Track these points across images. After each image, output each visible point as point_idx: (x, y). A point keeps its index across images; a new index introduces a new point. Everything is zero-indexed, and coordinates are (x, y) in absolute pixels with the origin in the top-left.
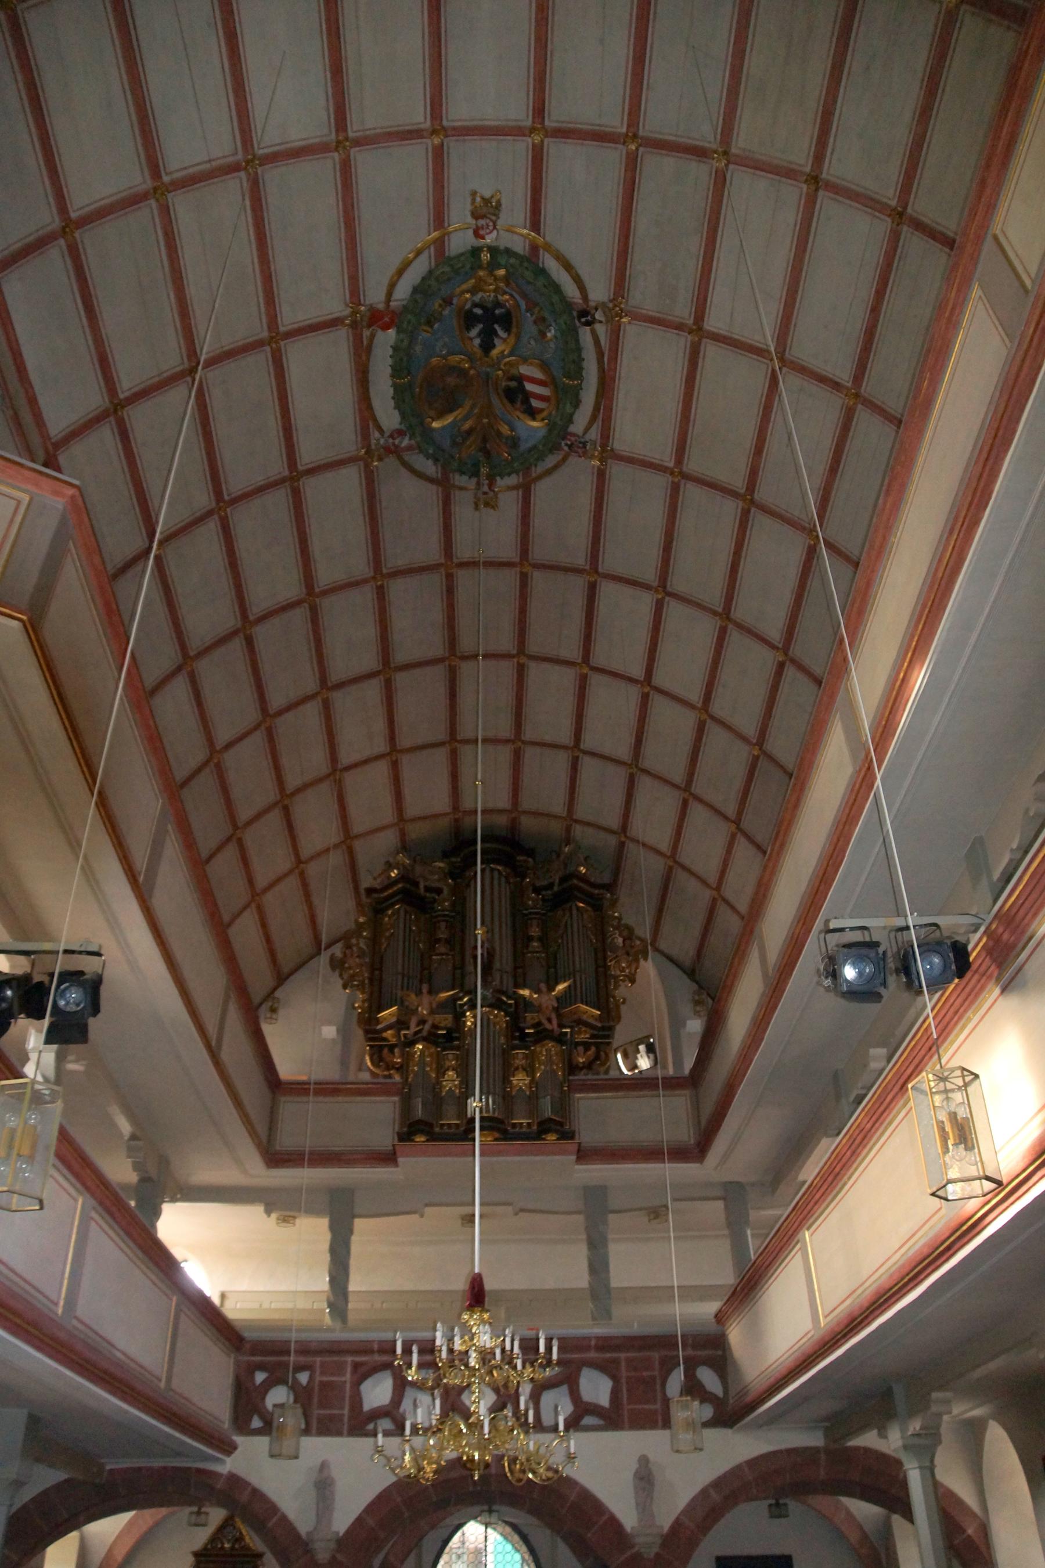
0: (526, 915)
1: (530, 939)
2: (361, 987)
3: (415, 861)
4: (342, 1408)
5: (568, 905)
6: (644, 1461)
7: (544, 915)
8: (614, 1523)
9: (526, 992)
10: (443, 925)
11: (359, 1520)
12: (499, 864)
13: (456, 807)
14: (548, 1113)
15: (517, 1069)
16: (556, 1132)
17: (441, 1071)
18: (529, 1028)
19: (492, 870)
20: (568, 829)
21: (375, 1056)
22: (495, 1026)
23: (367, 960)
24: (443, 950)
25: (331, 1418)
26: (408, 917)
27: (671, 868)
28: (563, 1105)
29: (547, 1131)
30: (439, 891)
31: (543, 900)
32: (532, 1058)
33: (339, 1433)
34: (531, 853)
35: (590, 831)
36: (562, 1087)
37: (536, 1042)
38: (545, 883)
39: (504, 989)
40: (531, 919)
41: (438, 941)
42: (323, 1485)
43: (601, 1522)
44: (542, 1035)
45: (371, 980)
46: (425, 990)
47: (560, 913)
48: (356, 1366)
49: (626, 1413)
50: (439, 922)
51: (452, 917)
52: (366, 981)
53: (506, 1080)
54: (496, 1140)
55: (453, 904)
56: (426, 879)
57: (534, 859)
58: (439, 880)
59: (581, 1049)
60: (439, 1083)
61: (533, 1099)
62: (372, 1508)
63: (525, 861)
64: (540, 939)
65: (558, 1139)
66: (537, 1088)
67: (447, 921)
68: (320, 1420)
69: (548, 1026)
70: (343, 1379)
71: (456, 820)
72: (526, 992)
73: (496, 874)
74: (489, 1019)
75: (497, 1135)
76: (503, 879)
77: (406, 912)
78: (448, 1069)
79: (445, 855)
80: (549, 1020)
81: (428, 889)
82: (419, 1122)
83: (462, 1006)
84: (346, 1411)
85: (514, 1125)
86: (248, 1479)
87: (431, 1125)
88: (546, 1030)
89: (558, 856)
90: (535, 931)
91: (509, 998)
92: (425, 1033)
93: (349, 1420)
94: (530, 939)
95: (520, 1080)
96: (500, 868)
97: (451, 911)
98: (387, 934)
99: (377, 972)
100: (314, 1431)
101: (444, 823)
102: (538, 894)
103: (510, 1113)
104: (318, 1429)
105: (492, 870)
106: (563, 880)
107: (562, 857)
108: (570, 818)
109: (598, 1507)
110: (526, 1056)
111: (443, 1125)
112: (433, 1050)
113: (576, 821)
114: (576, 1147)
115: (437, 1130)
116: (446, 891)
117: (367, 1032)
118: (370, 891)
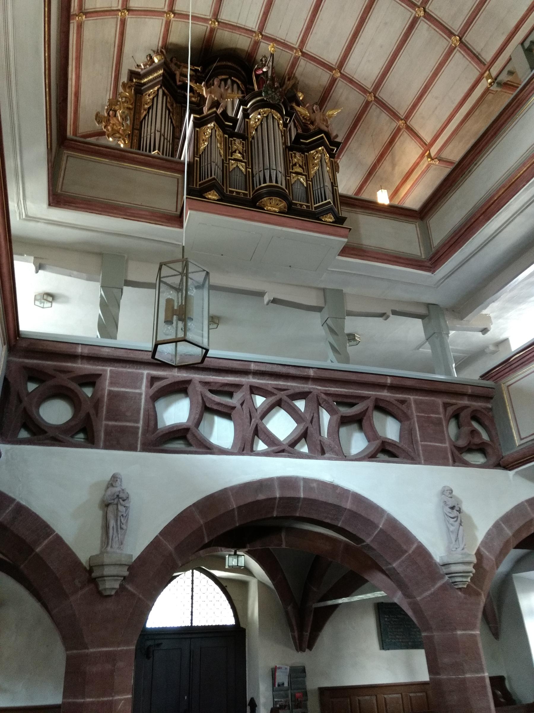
4: (137, 421)
6: (448, 492)
8: (422, 552)
11: (155, 545)
15: (295, 165)
17: (229, 151)
19: (233, 82)
25: (123, 430)
26: (165, 97)
27: (367, 104)
33: (132, 448)
42: (113, 504)
43: (410, 552)
48: (153, 380)
49: (420, 448)
62: (167, 532)
68: (108, 433)
70: (137, 391)
71: (212, 30)
77: (164, 94)
84: (141, 424)
86: (11, 495)
93: (144, 434)
96: (239, 82)
98: (146, 106)
99: (136, 132)
100: (102, 444)
104: (105, 442)
109: (406, 536)
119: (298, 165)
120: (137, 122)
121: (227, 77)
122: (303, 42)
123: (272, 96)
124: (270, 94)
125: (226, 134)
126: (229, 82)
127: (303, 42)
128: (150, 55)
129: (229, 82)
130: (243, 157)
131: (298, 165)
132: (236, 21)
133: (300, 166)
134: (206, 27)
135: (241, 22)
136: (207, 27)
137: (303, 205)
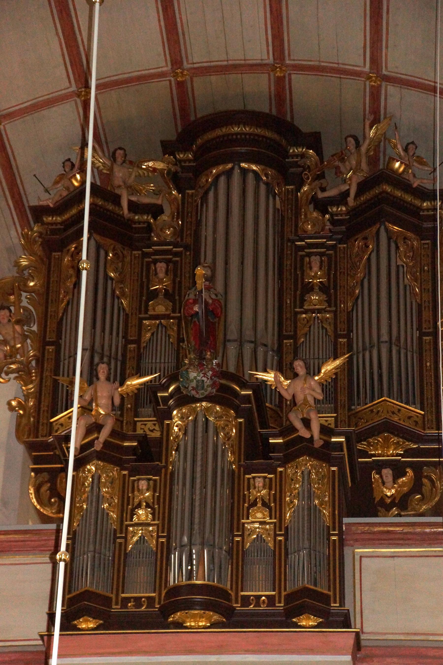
0: (301, 248)
1: (309, 289)
2: (24, 375)
3: (113, 158)
5: (374, 229)
7: (333, 247)
9: (270, 377)
10: (161, 267)
12: (256, 162)
13: (176, 63)
14: (303, 581)
15: (255, 504)
16: (316, 613)
17: (127, 509)
18: (275, 436)
20: (375, 95)
21: (45, 488)
22: (217, 434)
23: (35, 328)
24: (161, 309)
26: (102, 253)
28: (336, 568)
29: (300, 611)
30: (156, 211)
31: (333, 222)
32: (279, 488)
34: (314, 141)
35: (412, 96)
36: (329, 535)
37: (285, 461)
38: (332, 193)
39: (232, 369)
40: (309, 255)
41: (154, 295)
44: (298, 447)
45: (40, 361)
46: (102, 376)
47: (359, 243)
50: (155, 262)
51: (176, 254)
52: (34, 363)
53: (235, 525)
54: (213, 625)
55: (179, 233)
56: (132, 190)
57: (319, 152)
58: (156, 193)
59: (387, 473)
60: (123, 528)
61: (280, 556)
63: (303, 156)
64: (324, 289)
65: (319, 626)
66: (286, 535)
67: (168, 262)
69: (304, 433)
72: (270, 377)
73: (251, 176)
74: (207, 420)
75: (216, 617)
76: (263, 187)
78: (139, 506)
79: (168, 148)
80: (307, 423)
81: (134, 207)
82: (87, 595)
83: (165, 400)
85: (246, 601)
87: (107, 601)
88: (301, 439)
89: (358, 145)
90: (316, 274)
91: (244, 386)
92: (98, 446)
94: (309, 289)
95: (257, 522)
97: (176, 245)
99: (51, 348)
101: (162, 90)
102: (324, 212)
103: (239, 580)
105: (244, 172)
106: (363, 187)
107: (363, 149)
108: (378, 76)
110: (269, 485)
111: (128, 600)
112: (114, 472)
113: (388, 79)
114: (350, 641)
115: (116, 608)
116: (167, 209)
117: (31, 447)
118: (39, 212)
119: (259, 505)
120: (52, 325)
121: (230, 166)
122: (375, 61)
123: (198, 381)
124: (195, 378)
125: (125, 469)
126: (237, 171)
127: (375, 61)
128: (69, 160)
129: (237, 171)
130: (153, 514)
131: (259, 505)
132: (224, 57)
133: (264, 504)
134: (168, 83)
135: (236, 56)
136: (170, 81)
137: (262, 596)
